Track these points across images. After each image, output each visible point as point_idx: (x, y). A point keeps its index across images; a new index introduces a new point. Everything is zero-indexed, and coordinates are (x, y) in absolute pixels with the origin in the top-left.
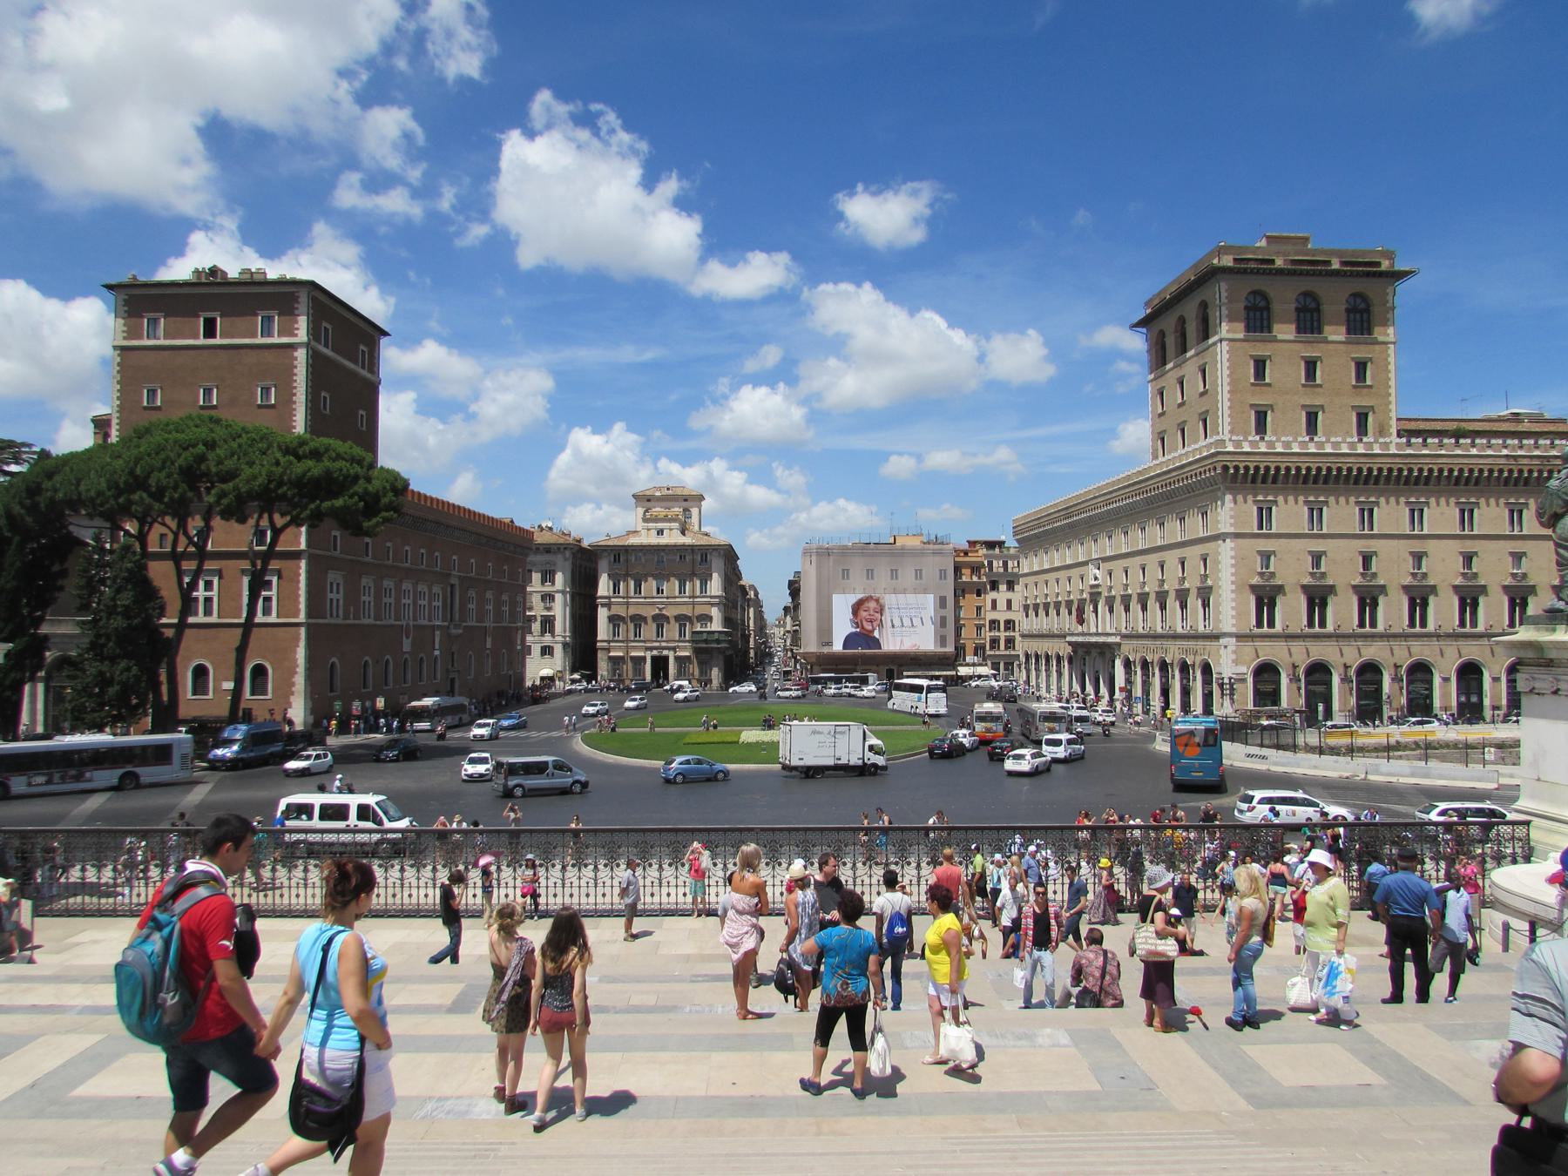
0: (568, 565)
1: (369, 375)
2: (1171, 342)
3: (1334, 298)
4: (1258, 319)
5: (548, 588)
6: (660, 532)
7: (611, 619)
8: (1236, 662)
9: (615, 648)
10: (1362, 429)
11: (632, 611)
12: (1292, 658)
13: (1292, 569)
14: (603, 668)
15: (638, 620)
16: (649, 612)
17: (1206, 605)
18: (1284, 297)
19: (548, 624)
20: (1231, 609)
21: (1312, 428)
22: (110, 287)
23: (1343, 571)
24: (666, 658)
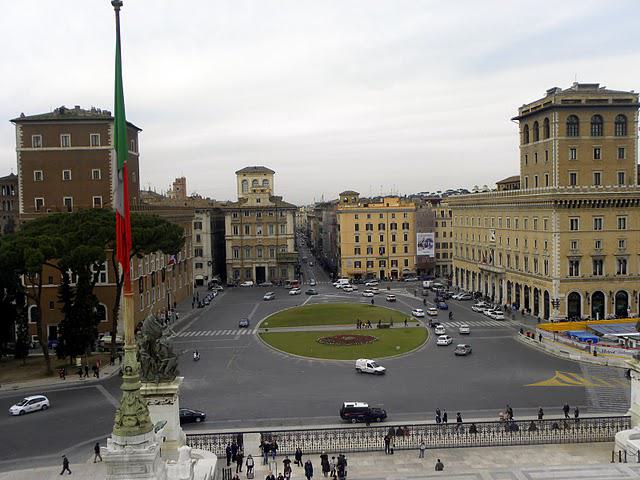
0: (209, 218)
1: (134, 153)
2: (531, 133)
3: (609, 119)
4: (573, 127)
5: (198, 232)
6: (258, 201)
7: (232, 247)
8: (560, 292)
10: (621, 182)
12: (585, 289)
13: (586, 249)
14: (230, 274)
15: (248, 248)
17: (546, 263)
18: (586, 119)
19: (199, 252)
20: (558, 267)
21: (597, 183)
22: (12, 121)
23: (610, 248)
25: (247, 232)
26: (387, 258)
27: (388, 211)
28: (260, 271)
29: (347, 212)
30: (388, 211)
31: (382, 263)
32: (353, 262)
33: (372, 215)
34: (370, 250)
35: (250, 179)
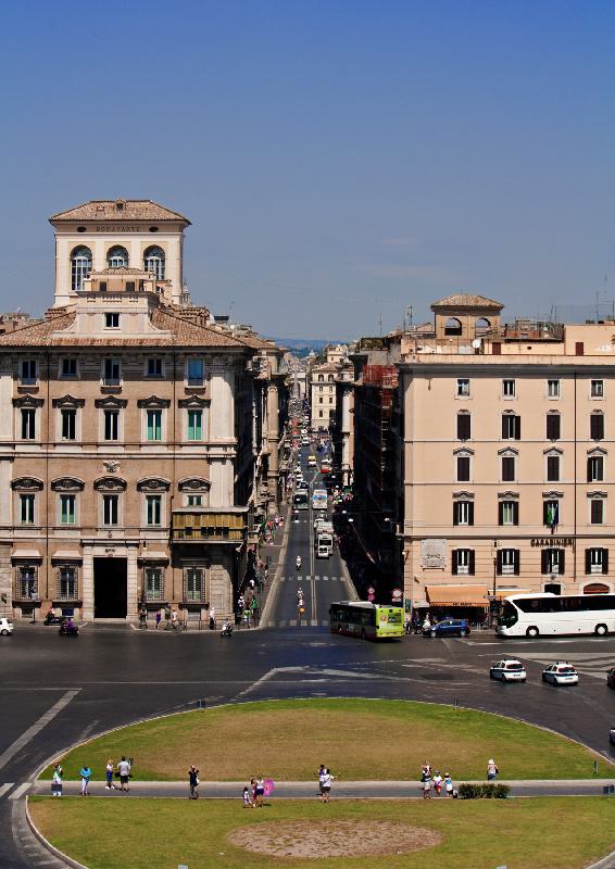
6: (112, 319)
9: (25, 542)
11: (57, 472)
15: (68, 489)
16: (90, 474)
24: (123, 562)
25: (69, 430)
26: (570, 540)
27: (576, 372)
28: (110, 574)
29: (432, 371)
30: (576, 372)
31: (552, 559)
32: (445, 550)
33: (519, 383)
34: (509, 507)
35: (100, 245)
